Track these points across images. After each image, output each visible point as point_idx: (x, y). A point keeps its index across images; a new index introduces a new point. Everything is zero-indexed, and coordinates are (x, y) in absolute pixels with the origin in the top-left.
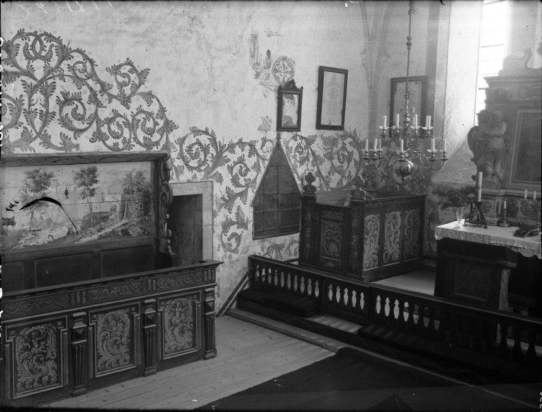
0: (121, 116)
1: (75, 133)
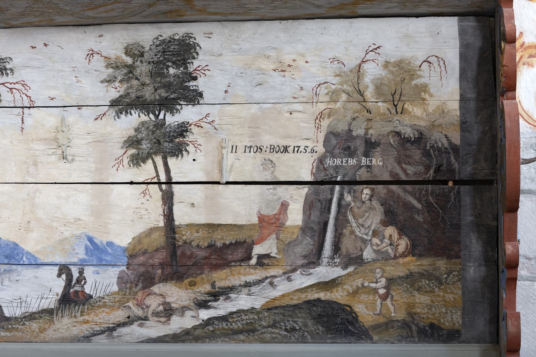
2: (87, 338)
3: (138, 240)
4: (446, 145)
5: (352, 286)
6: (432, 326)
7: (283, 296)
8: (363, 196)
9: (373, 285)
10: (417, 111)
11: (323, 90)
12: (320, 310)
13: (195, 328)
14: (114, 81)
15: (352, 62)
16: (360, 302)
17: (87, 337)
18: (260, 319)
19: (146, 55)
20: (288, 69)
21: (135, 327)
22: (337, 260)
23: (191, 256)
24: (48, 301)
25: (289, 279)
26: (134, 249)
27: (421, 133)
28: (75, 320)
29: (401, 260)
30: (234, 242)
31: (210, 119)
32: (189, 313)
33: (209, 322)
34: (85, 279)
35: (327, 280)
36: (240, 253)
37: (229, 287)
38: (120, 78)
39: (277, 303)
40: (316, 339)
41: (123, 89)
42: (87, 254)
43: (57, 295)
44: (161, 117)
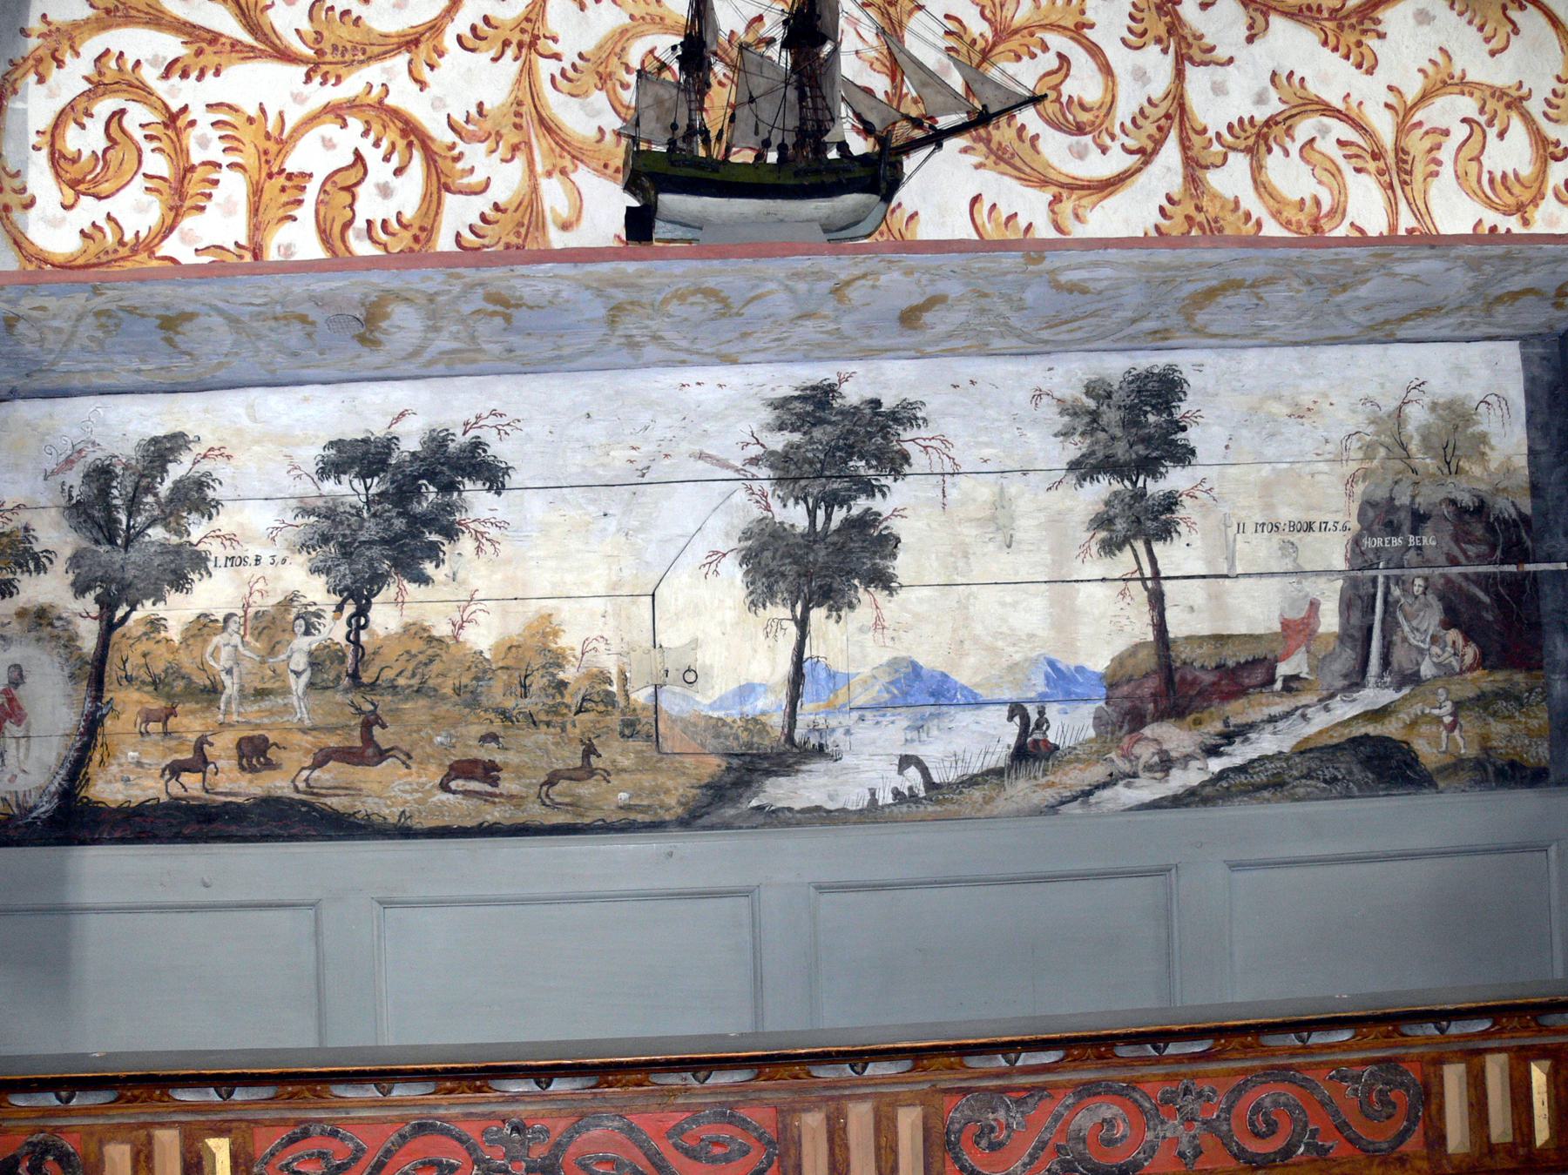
0: (1327, 110)
1: (1057, 199)
2: (1053, 809)
3: (1119, 661)
4: (1514, 515)
5: (1408, 714)
6: (1512, 764)
7: (1320, 732)
8: (1416, 588)
9: (1436, 712)
10: (1477, 470)
11: (1354, 444)
12: (1368, 749)
13: (1203, 785)
14: (1073, 434)
15: (1389, 404)
16: (1420, 736)
17: (1053, 807)
18: (1290, 768)
19: (1115, 397)
20: (1308, 414)
21: (1120, 788)
22: (1388, 679)
23: (1195, 681)
24: (995, 757)
25: (1327, 709)
26: (1114, 675)
27: (1482, 502)
28: (1035, 782)
29: (1469, 676)
30: (1250, 659)
31: (1207, 486)
32: (1194, 764)
33: (1223, 775)
34: (1047, 721)
35: (1377, 707)
36: (1259, 675)
37: (1247, 724)
38: (1080, 430)
39: (1311, 745)
40: (1366, 791)
41: (1086, 445)
42: (1048, 685)
43: (1009, 747)
44: (1140, 484)
